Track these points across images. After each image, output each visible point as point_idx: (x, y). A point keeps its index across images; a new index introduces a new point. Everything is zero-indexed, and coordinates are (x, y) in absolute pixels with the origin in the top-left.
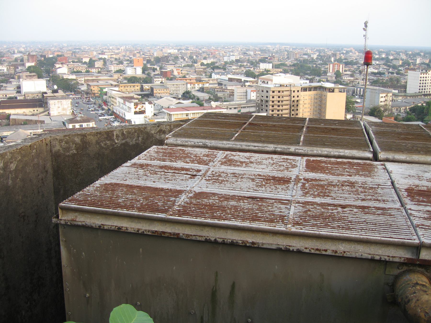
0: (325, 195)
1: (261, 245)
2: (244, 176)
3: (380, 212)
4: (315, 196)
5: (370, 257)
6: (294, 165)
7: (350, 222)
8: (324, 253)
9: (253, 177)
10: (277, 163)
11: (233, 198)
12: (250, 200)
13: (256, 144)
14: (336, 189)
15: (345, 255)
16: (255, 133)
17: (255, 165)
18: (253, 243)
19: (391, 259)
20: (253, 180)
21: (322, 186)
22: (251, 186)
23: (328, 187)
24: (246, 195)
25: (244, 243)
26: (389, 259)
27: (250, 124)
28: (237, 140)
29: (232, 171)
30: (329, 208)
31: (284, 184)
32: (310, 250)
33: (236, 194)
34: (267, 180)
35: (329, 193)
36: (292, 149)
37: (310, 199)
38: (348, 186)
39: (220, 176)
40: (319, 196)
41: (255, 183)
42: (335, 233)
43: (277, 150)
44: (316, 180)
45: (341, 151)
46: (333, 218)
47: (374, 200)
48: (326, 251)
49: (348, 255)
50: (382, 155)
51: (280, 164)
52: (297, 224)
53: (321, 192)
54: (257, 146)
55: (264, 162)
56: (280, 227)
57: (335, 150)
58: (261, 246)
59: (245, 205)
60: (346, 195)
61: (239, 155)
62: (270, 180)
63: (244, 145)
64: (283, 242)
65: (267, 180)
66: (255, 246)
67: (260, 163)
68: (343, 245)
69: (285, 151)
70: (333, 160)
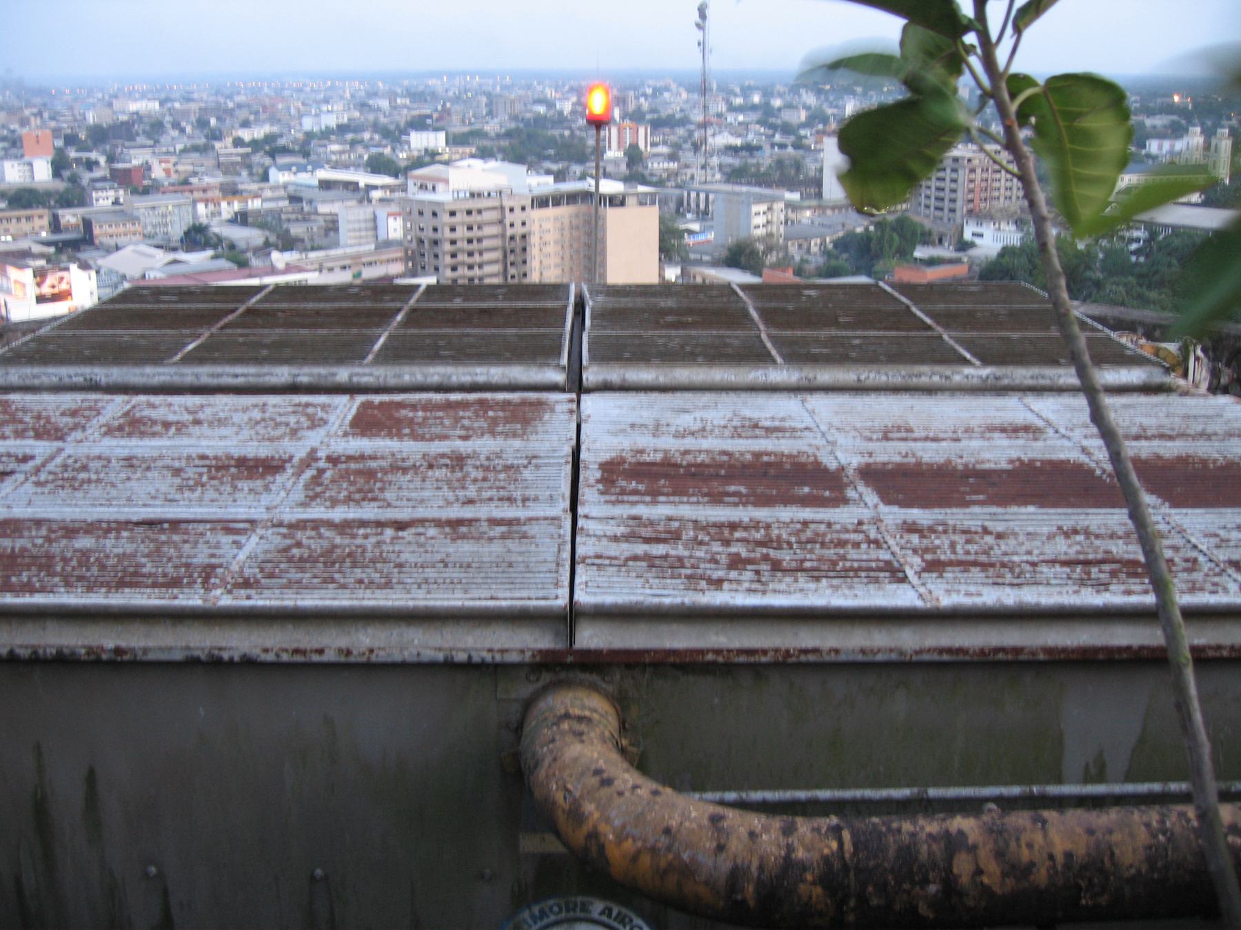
0: (367, 496)
1: (140, 653)
2: (160, 463)
3: (500, 529)
4: (334, 503)
5: (440, 657)
6: (322, 419)
7: (400, 565)
8: (316, 658)
9: (177, 464)
10: (272, 419)
11: (91, 528)
12: (141, 529)
13: (239, 370)
14: (408, 477)
15: (374, 658)
16: (252, 338)
17: (205, 429)
18: (118, 651)
19: (498, 658)
20: (177, 472)
21: (370, 474)
22: (164, 488)
23: (386, 473)
24: (135, 518)
25: (93, 653)
26: (493, 658)
27: (249, 311)
28: (189, 360)
29: (125, 453)
30: (361, 531)
31: (263, 476)
32: (277, 655)
33: (106, 517)
34: (218, 468)
35: (382, 490)
36: (343, 374)
37: (317, 512)
38: (447, 466)
39: (85, 468)
40: (349, 500)
41: (178, 481)
42: (343, 601)
43: (301, 382)
44: (362, 457)
45: (479, 370)
46: (354, 559)
47: (501, 499)
48: (320, 651)
49: (381, 657)
50: (591, 375)
51: (279, 419)
52: (246, 584)
53: (359, 491)
54: (244, 375)
55: (238, 418)
56: (192, 599)
57: (461, 370)
58: (140, 657)
59: (114, 546)
60: (426, 494)
61: (170, 405)
62: (227, 467)
63: (204, 374)
64: (201, 641)
65: (218, 468)
66: (126, 658)
67: (222, 422)
68: (370, 631)
69: (323, 382)
70: (455, 397)
